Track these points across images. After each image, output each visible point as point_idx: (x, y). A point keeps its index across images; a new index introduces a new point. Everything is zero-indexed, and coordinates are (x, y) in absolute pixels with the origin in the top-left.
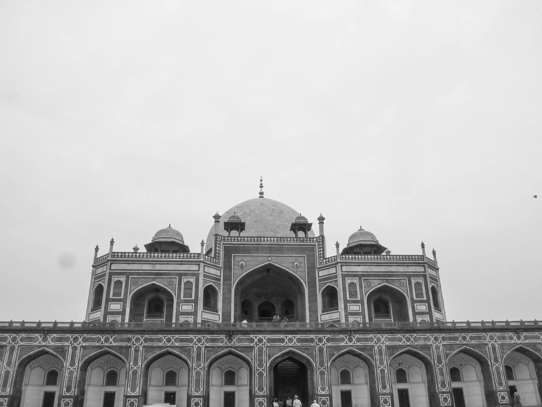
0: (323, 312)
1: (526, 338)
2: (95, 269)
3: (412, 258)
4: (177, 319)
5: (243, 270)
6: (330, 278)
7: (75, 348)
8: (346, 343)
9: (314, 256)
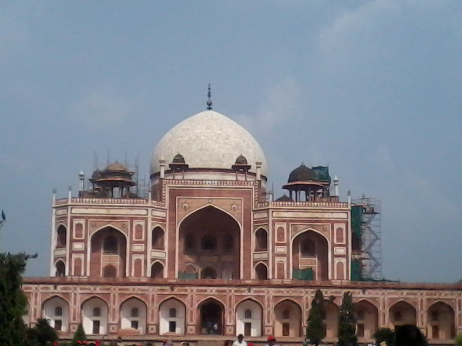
0: (256, 251)
1: (369, 293)
5: (187, 213)
6: (262, 222)
7: (75, 294)
9: (250, 199)
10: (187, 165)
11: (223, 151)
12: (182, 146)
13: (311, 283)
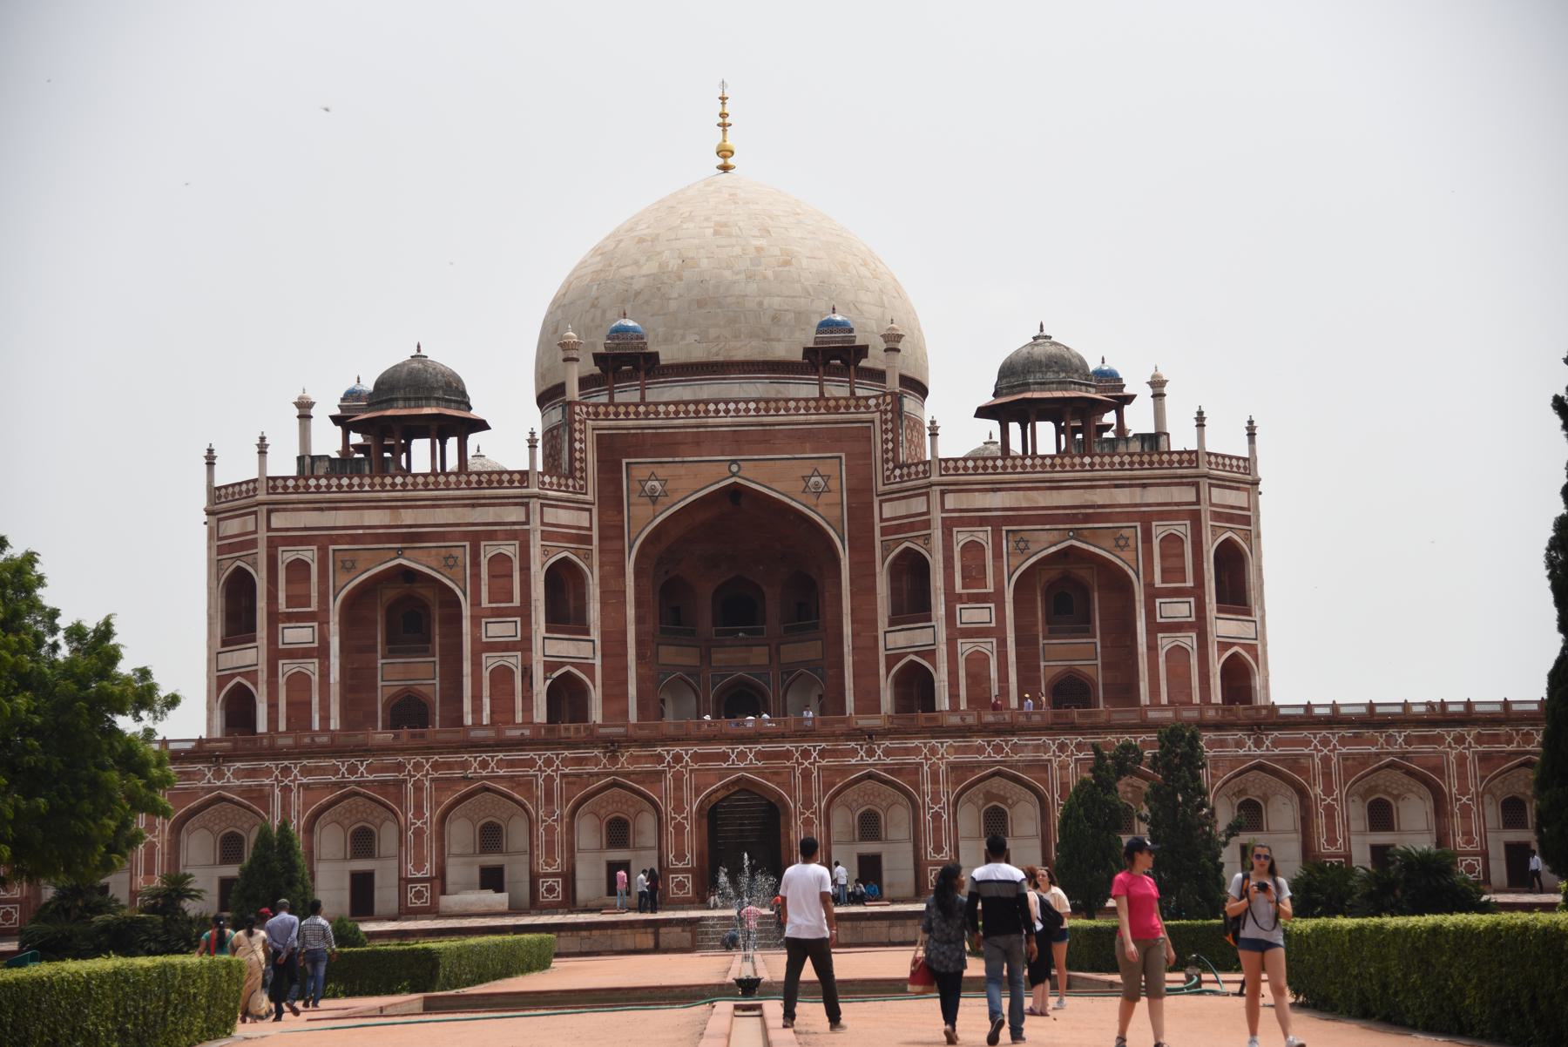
0: (892, 623)
1: (1275, 743)
2: (214, 519)
3: (1161, 462)
4: (477, 665)
5: (659, 508)
6: (912, 527)
7: (286, 790)
8: (861, 758)
9: (868, 455)
10: (655, 355)
11: (776, 302)
12: (637, 294)
13: (1075, 714)
